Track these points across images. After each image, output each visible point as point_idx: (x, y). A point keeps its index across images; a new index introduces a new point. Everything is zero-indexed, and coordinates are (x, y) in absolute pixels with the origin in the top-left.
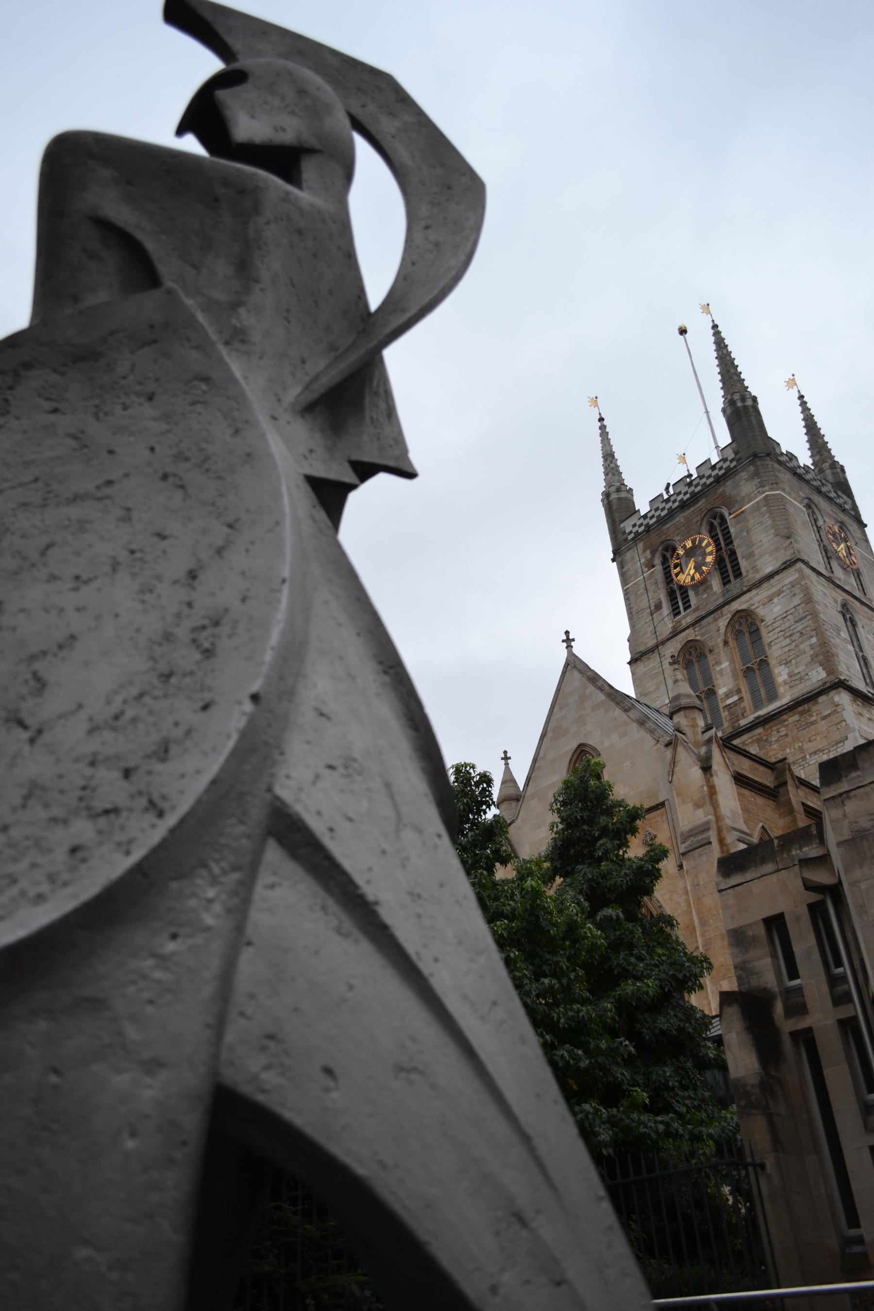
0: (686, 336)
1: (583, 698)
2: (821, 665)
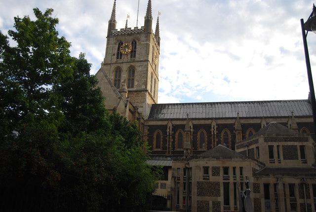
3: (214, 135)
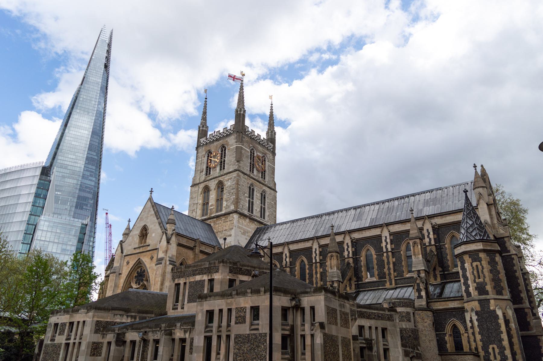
3: (316, 263)
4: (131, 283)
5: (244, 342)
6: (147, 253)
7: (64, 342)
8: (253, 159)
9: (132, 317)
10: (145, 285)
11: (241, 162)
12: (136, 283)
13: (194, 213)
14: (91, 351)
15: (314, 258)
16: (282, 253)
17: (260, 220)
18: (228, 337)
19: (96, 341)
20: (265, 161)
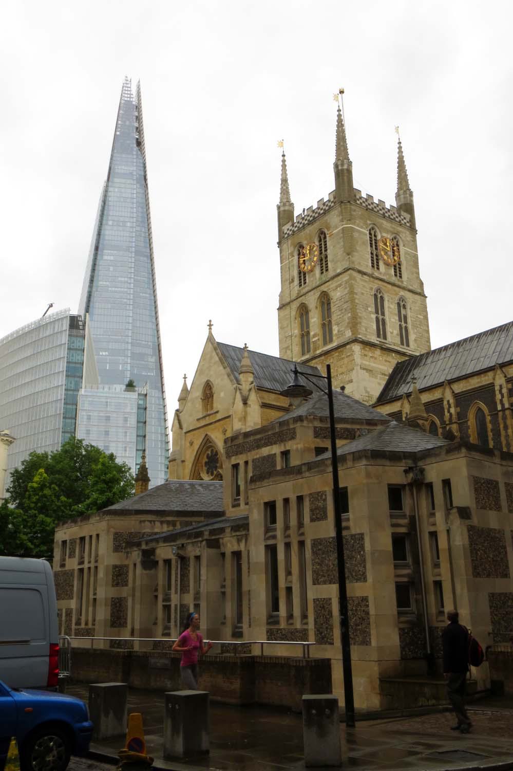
0: (343, 95)
1: (211, 358)
2: (351, 329)
3: (504, 410)
4: (200, 474)
5: (328, 552)
6: (217, 424)
7: (76, 567)
8: (376, 246)
9: (168, 523)
10: (220, 474)
11: (355, 253)
12: (208, 473)
13: (289, 352)
14: (113, 579)
15: (498, 402)
16: (441, 400)
17: (401, 349)
18: (302, 544)
19: (118, 563)
20: (398, 245)
